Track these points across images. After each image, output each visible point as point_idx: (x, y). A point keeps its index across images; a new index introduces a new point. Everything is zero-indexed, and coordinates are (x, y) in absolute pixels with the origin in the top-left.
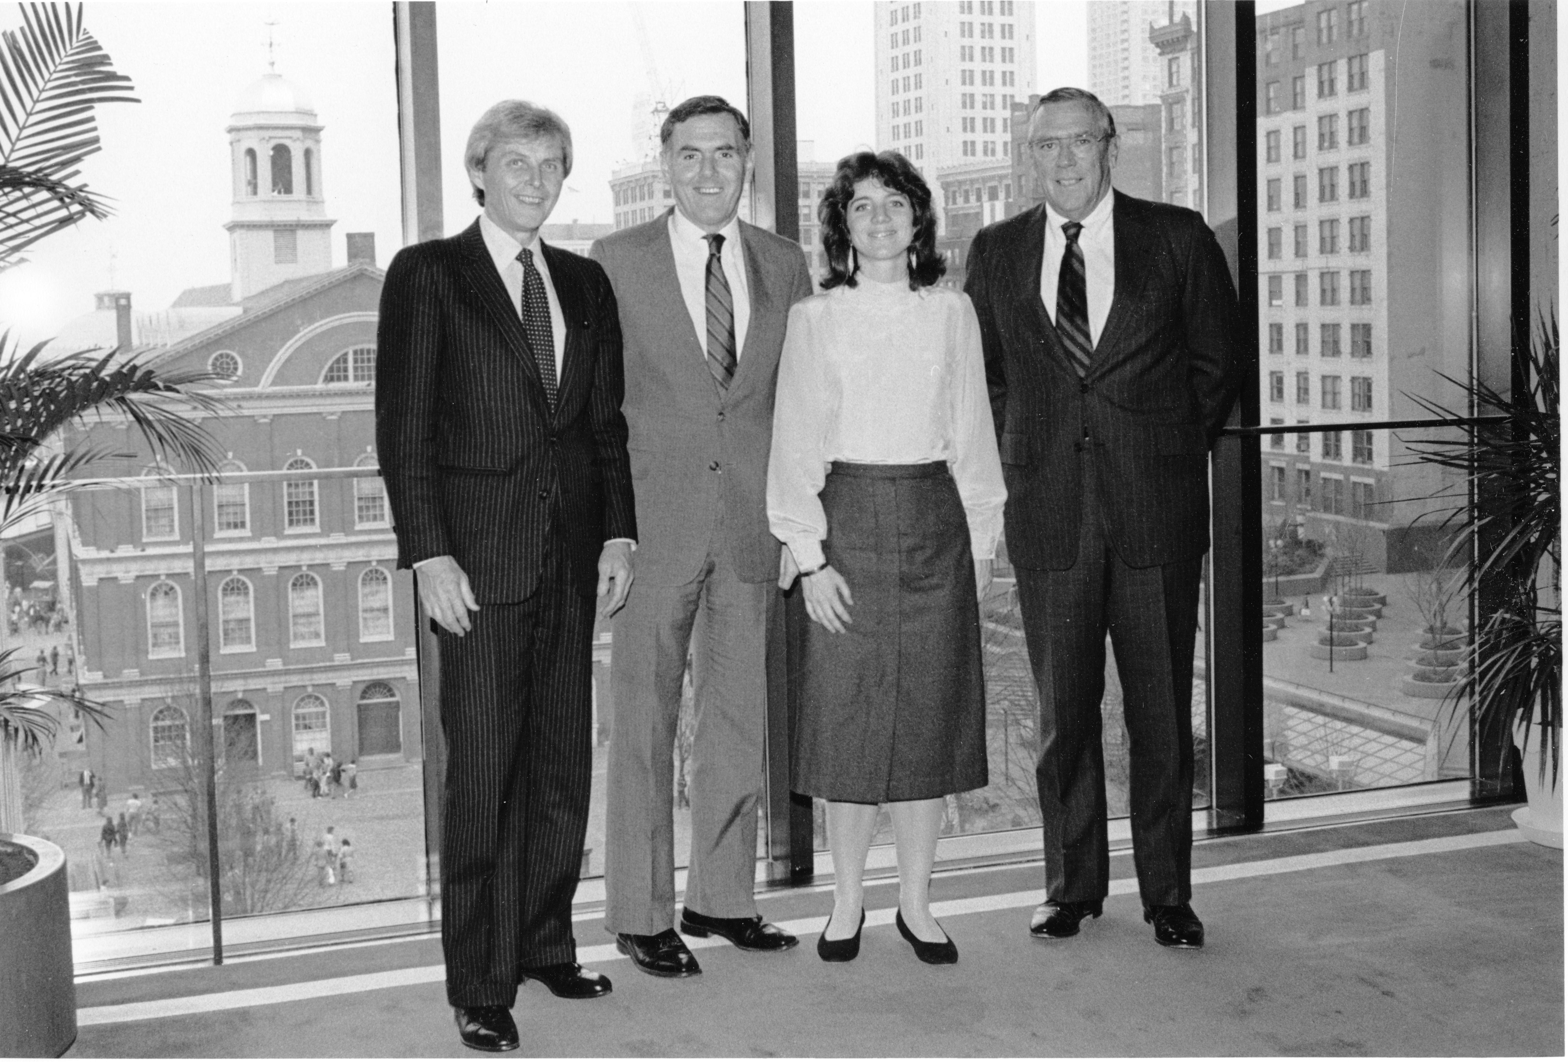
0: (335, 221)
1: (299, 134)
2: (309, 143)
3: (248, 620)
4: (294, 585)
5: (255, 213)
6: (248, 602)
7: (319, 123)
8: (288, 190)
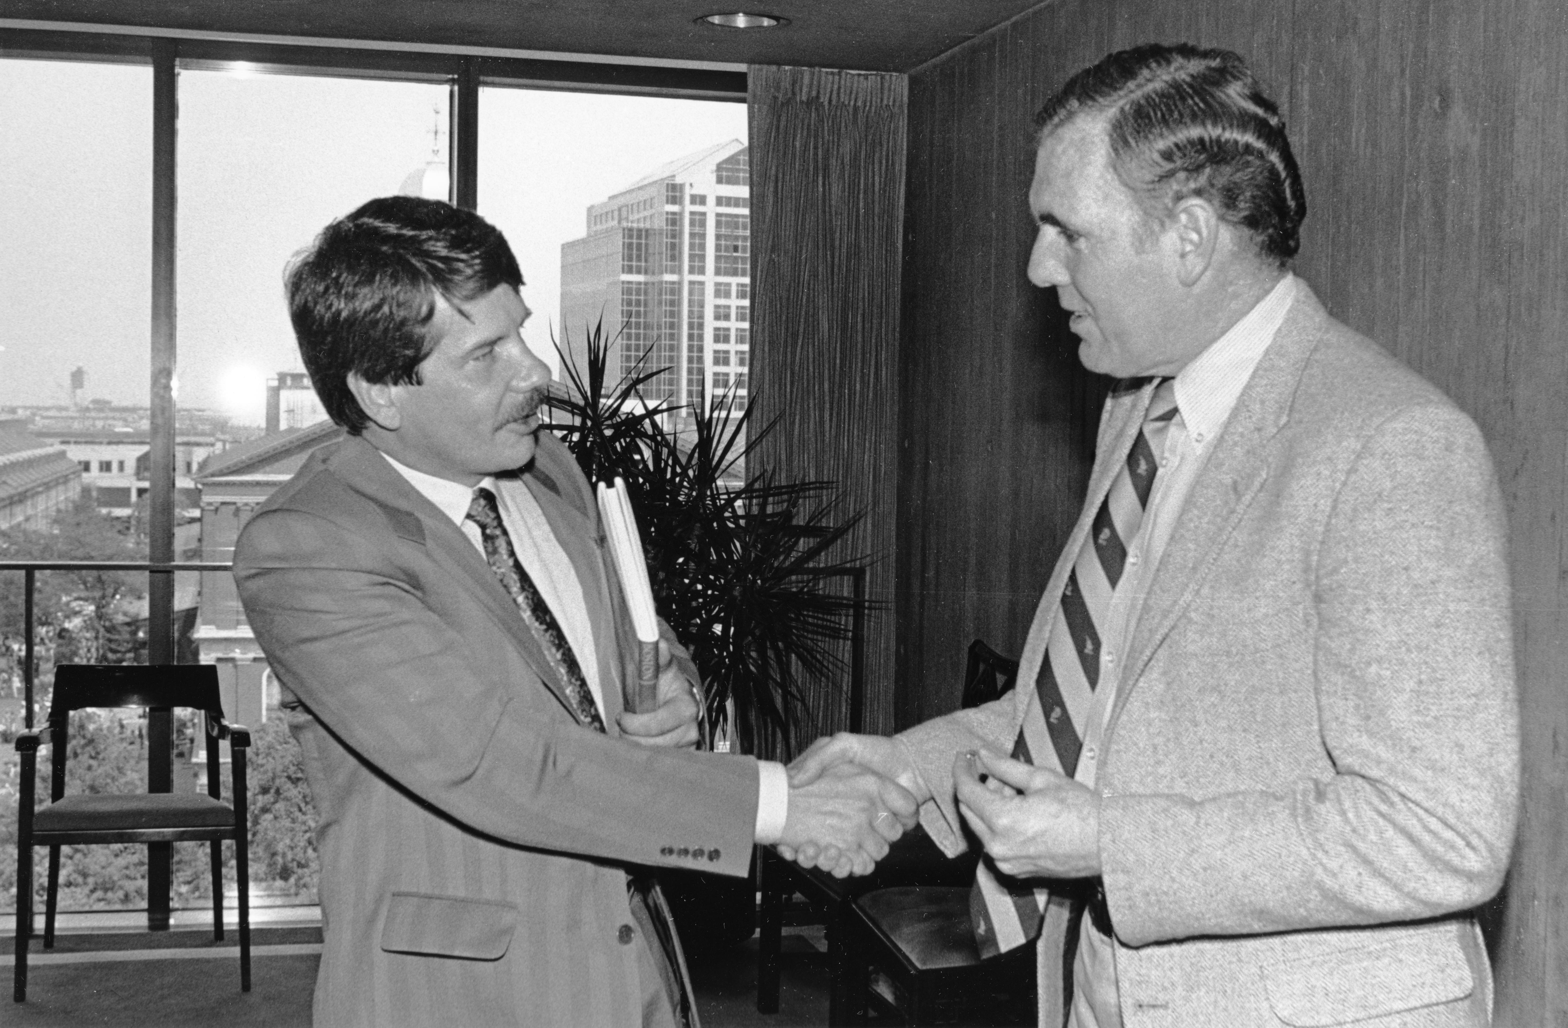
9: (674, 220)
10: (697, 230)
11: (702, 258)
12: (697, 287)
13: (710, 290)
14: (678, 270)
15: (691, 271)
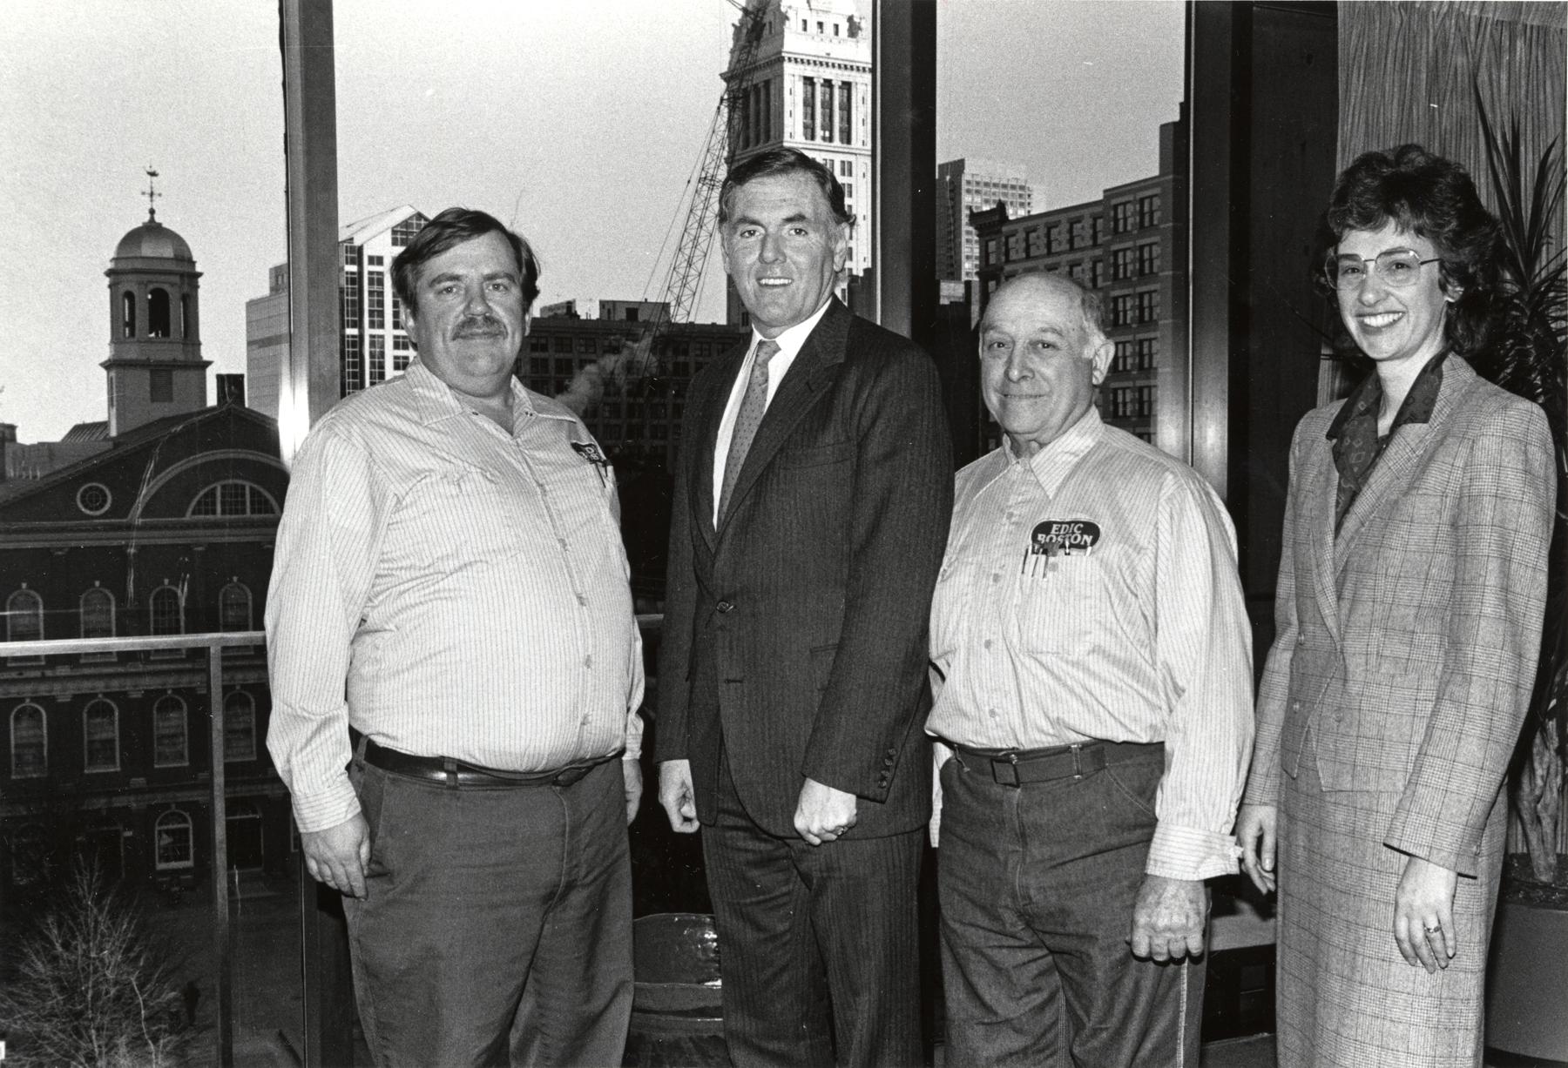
0: (209, 363)
1: (176, 279)
2: (186, 289)
3: (112, 741)
4: (159, 709)
5: (132, 353)
6: (112, 723)
7: (198, 269)
8: (166, 333)
9: (356, 279)
10: (376, 288)
11: (381, 314)
12: (377, 342)
13: (389, 344)
14: (359, 324)
15: (372, 325)
